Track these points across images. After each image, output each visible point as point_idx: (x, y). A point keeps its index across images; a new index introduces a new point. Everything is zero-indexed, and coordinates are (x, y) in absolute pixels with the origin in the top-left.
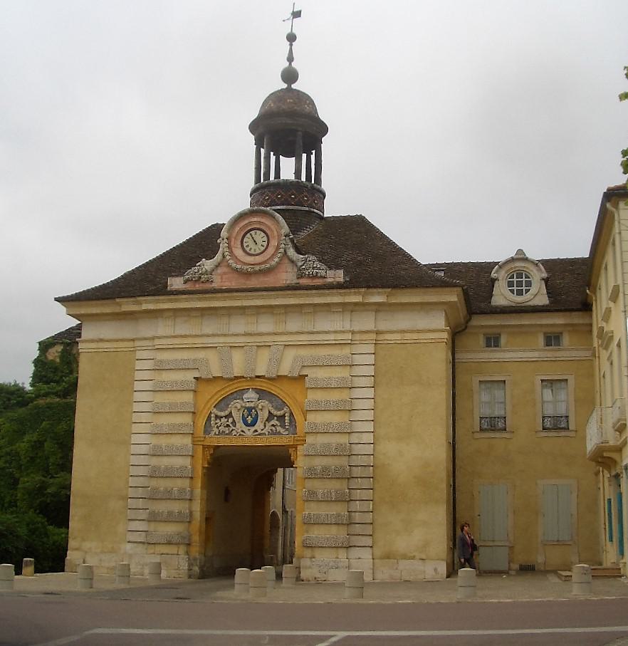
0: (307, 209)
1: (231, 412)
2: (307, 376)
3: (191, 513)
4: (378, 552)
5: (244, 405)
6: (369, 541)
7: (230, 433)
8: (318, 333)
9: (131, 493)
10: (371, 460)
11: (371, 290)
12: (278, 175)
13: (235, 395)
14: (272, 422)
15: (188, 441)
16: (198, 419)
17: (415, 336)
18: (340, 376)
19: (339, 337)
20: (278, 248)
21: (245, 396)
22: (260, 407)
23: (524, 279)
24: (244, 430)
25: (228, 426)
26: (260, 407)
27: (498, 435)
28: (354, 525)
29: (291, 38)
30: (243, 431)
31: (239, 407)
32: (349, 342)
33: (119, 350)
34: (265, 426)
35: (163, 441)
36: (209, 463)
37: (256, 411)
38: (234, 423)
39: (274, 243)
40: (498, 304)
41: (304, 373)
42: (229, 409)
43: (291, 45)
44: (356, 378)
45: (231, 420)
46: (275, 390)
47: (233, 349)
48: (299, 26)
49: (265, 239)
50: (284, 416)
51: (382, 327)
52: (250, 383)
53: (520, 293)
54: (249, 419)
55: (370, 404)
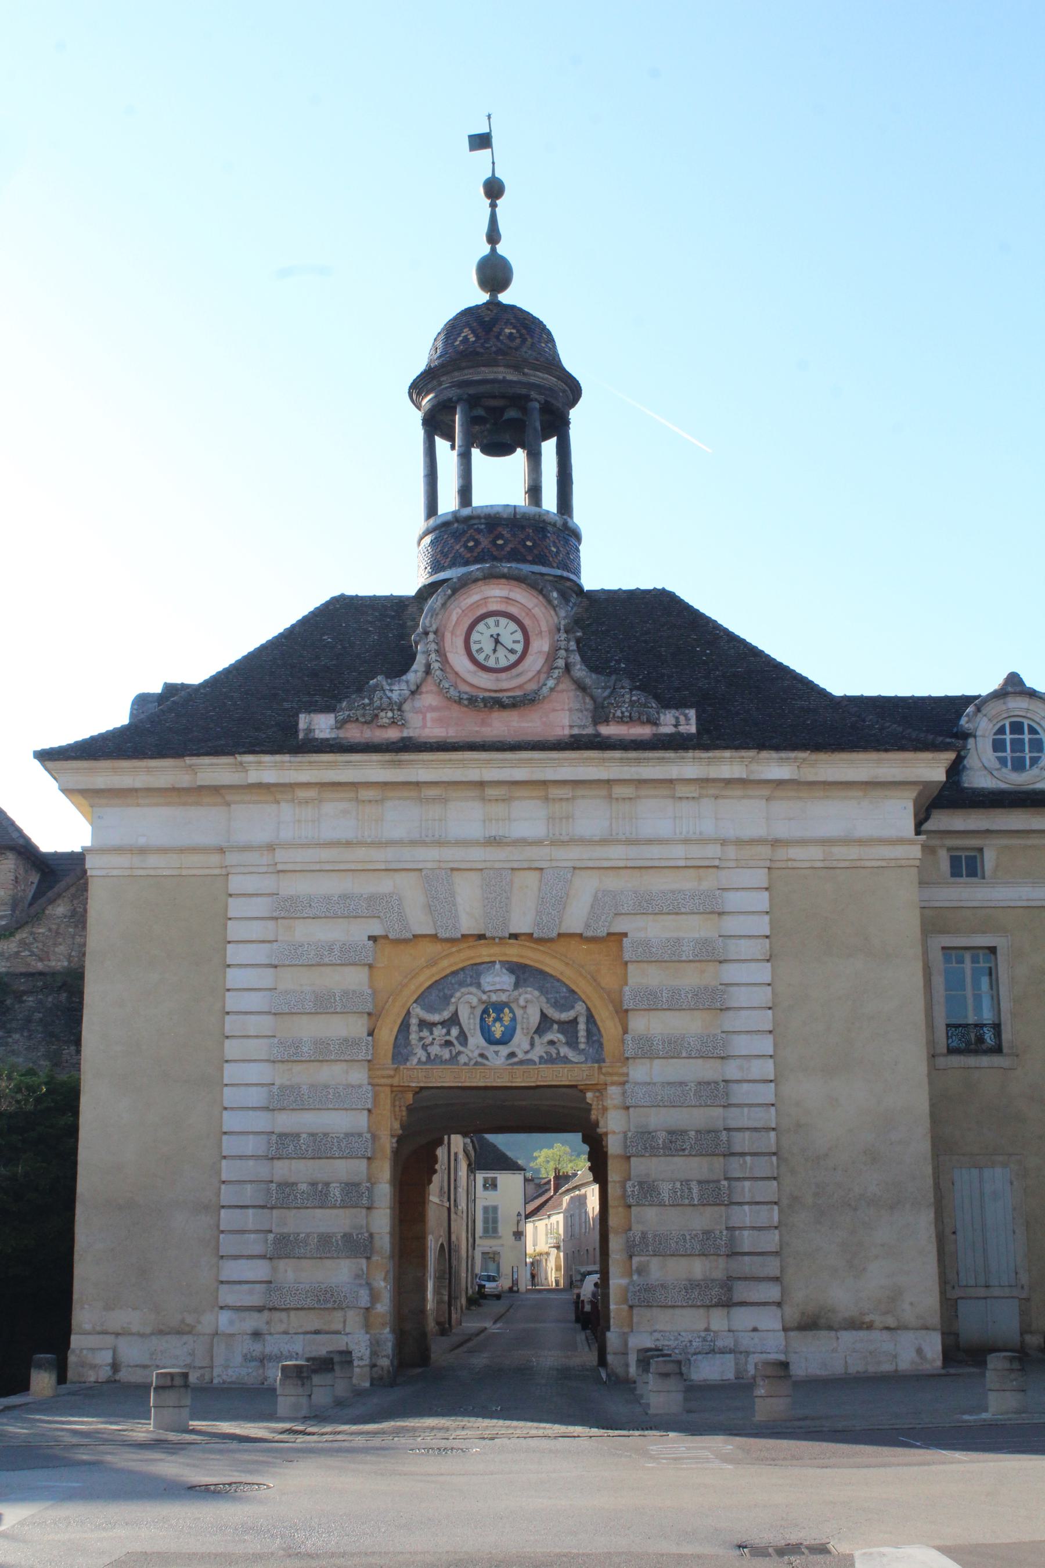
0: (559, 572)
1: (456, 1014)
2: (625, 935)
4: (792, 1313)
5: (484, 997)
6: (773, 1292)
7: (454, 1059)
8: (650, 842)
9: (227, 1195)
10: (770, 1117)
11: (764, 754)
12: (465, 492)
13: (461, 976)
14: (550, 1036)
15: (359, 1076)
17: (853, 853)
20: (551, 657)
22: (522, 1002)
23: (1026, 737)
24: (486, 1053)
25: (448, 1043)
27: (985, 1061)
28: (740, 1258)
29: (494, 189)
30: (482, 1055)
31: (474, 1001)
32: (716, 863)
33: (184, 872)
35: (302, 1075)
36: (402, 1127)
37: (512, 1011)
38: (463, 1038)
39: (541, 645)
40: (976, 785)
43: (493, 206)
45: (455, 1032)
46: (551, 965)
47: (455, 873)
49: (519, 636)
50: (575, 1021)
51: (782, 830)
53: (1019, 766)
54: (498, 1030)
55: (764, 996)
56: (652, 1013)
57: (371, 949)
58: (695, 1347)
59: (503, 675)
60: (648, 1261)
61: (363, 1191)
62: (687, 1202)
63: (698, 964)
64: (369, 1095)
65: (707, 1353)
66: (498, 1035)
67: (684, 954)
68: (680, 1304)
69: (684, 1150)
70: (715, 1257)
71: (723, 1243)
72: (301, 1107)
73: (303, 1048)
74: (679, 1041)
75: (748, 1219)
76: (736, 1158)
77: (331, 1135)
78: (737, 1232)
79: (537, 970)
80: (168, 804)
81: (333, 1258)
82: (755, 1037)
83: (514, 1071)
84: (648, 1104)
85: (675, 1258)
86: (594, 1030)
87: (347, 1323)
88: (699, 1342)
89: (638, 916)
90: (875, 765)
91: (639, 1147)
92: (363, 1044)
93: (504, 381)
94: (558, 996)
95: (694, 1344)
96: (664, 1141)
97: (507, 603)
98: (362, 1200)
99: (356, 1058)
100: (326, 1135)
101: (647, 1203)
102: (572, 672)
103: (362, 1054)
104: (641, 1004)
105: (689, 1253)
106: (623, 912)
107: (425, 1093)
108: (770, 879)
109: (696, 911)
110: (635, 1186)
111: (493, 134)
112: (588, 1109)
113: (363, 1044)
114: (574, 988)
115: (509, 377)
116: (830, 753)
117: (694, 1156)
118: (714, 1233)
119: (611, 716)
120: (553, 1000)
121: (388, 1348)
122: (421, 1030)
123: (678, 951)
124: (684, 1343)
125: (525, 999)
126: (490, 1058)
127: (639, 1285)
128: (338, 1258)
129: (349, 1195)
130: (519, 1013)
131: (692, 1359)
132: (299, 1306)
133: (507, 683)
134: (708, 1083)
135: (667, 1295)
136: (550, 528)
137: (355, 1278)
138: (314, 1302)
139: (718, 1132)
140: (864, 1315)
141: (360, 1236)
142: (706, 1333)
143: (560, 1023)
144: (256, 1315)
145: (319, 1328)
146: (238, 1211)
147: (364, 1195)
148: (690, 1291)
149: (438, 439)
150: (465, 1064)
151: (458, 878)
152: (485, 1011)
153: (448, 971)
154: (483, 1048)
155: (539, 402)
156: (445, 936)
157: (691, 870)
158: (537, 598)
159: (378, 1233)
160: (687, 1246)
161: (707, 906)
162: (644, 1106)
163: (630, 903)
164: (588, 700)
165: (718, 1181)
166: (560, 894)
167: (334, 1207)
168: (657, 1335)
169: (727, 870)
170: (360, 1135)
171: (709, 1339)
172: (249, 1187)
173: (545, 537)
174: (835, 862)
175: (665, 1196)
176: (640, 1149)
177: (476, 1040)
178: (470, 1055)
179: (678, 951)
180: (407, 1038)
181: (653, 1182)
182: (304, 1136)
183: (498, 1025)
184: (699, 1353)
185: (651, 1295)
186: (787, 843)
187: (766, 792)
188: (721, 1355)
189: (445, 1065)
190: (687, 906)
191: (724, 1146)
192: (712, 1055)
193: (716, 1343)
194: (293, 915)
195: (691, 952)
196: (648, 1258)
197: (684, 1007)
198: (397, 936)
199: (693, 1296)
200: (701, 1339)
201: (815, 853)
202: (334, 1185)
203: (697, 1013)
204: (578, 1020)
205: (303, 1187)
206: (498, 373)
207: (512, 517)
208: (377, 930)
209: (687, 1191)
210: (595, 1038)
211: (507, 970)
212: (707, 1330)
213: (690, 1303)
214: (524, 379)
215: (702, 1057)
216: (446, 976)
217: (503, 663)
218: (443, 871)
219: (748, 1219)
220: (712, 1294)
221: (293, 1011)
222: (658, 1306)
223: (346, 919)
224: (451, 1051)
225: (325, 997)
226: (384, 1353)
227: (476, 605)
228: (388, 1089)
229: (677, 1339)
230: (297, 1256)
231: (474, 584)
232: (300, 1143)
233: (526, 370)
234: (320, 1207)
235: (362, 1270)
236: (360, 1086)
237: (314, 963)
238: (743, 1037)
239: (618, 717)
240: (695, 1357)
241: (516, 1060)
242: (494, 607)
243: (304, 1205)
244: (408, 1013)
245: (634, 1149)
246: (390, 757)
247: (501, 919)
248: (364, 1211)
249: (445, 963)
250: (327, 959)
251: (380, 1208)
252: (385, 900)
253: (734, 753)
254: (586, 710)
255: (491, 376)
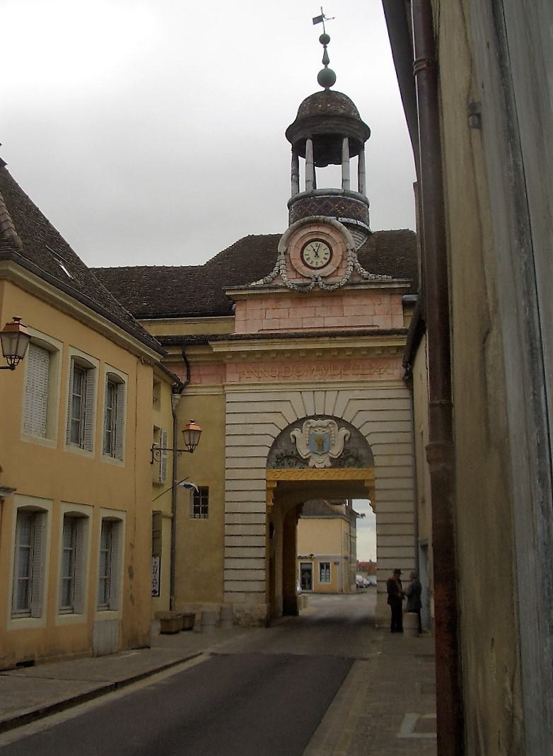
29: (325, 40)
43: (325, 47)
48: (329, 27)
149: (299, 157)
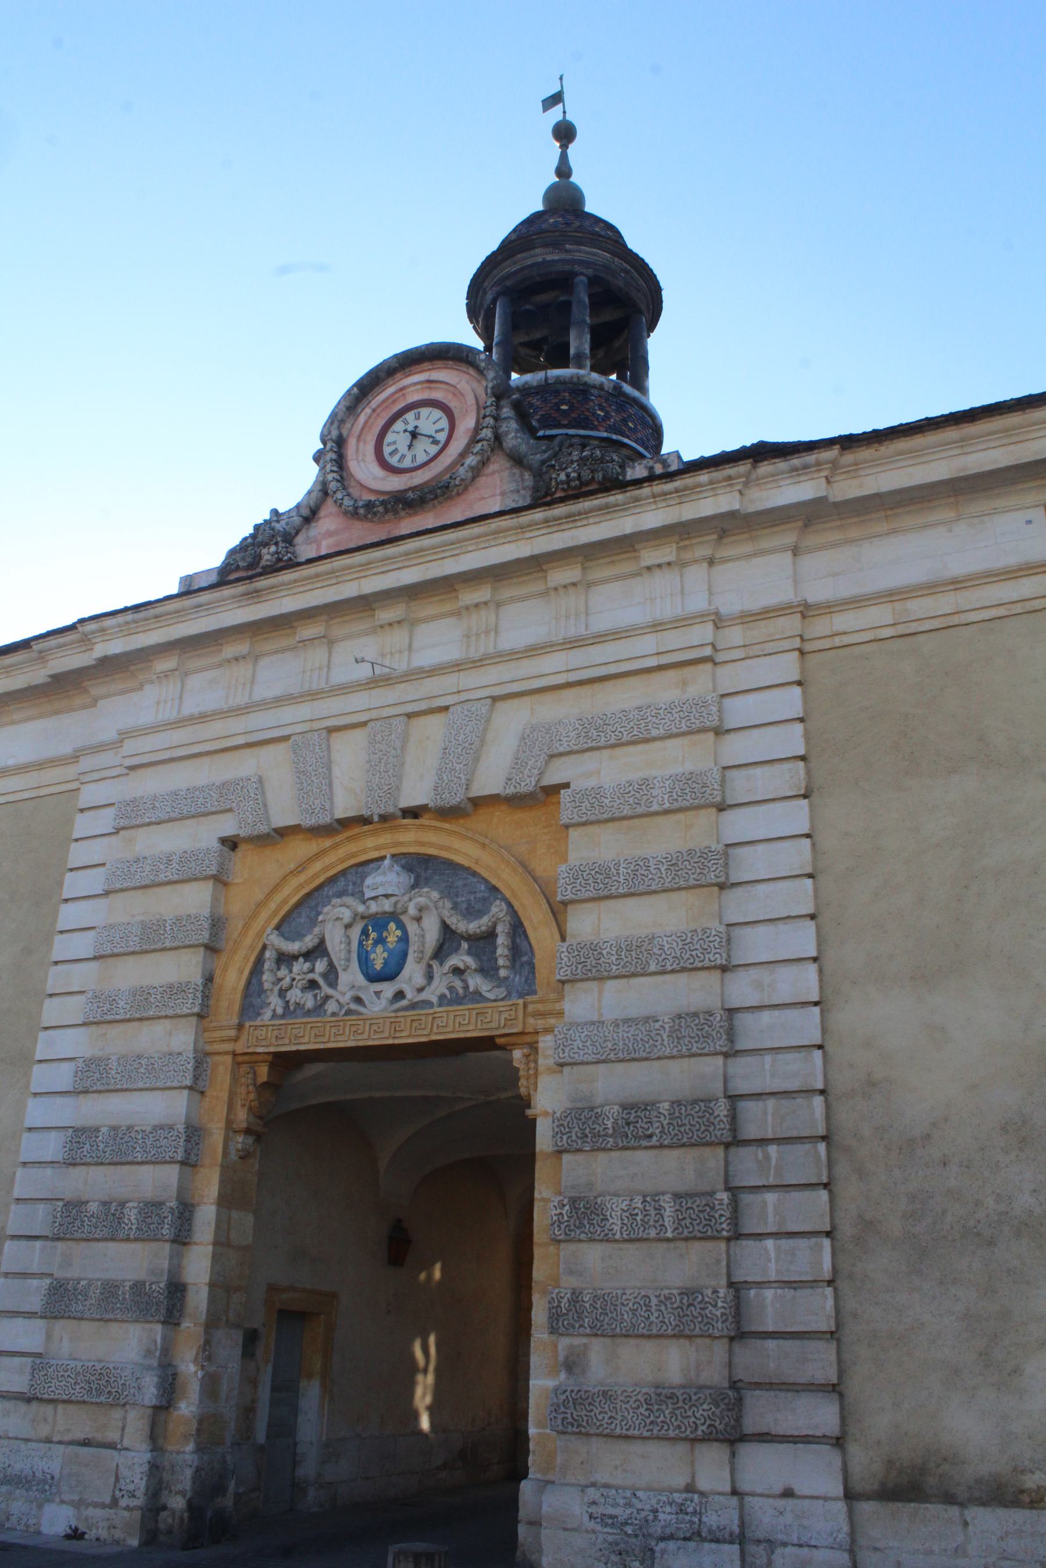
2: (567, 786)
3: (177, 1289)
5: (361, 908)
7: (319, 1008)
8: (601, 638)
9: (16, 1220)
13: (341, 883)
14: (454, 961)
16: (225, 970)
17: (945, 603)
18: (680, 770)
19: (673, 639)
20: (477, 429)
21: (369, 881)
22: (412, 911)
25: (313, 985)
26: (412, 911)
28: (758, 1343)
29: (565, 133)
33: (43, 792)
34: (430, 977)
38: (331, 975)
39: (467, 423)
41: (552, 778)
42: (316, 930)
44: (743, 773)
45: (321, 966)
47: (335, 735)
49: (444, 423)
50: (490, 935)
51: (817, 592)
52: (385, 838)
54: (379, 958)
56: (605, 905)
57: (216, 855)
58: (663, 1523)
59: (420, 472)
60: (585, 1345)
61: (166, 1214)
62: (653, 1233)
63: (680, 817)
64: (189, 1066)
65: (685, 1539)
66: (378, 966)
67: (655, 800)
68: (636, 1432)
69: (650, 1136)
70: (707, 1341)
71: (718, 1313)
72: (106, 1087)
73: (120, 1001)
74: (646, 944)
75: (772, 1265)
76: (752, 1149)
77: (136, 1128)
78: (752, 1292)
79: (444, 863)
80: (41, 716)
81: (116, 1320)
82: (781, 926)
83: (399, 1020)
84: (590, 1059)
85: (632, 1341)
86: (524, 946)
87: (127, 1431)
88: (669, 1513)
89: (588, 754)
90: (959, 451)
91: (573, 1135)
92: (191, 991)
93: (544, 262)
94: (472, 898)
95: (661, 1516)
96: (615, 1122)
97: (430, 388)
98: (162, 1228)
99: (179, 1012)
100: (129, 1128)
101: (583, 1236)
102: (504, 444)
103: (188, 1005)
104: (583, 890)
105: (654, 1332)
106: (561, 749)
107: (313, 1069)
108: (803, 670)
109: (675, 731)
110: (564, 1206)
111: (564, 90)
112: (513, 1076)
113: (191, 991)
114: (494, 882)
115: (549, 258)
116: (876, 445)
117: (669, 1147)
118: (703, 1296)
119: (553, 483)
120: (464, 906)
121: (185, 1480)
122: (279, 969)
123: (645, 797)
124: (643, 1514)
125: (416, 904)
126: (366, 1002)
127: (565, 1391)
128: (123, 1321)
129: (147, 1220)
130: (412, 928)
131: (657, 1549)
132: (65, 1397)
133: (420, 478)
134: (695, 1015)
135: (613, 1414)
136: (595, 392)
137: (145, 1356)
138: (84, 1391)
139: (710, 1101)
140: (1023, 1472)
141: (154, 1287)
142: (684, 1495)
143: (470, 938)
144: (22, 1407)
145: (90, 1436)
146: (24, 1243)
147: (166, 1221)
148: (656, 1407)
150: (334, 1014)
151: (338, 741)
152: (365, 933)
153: (322, 879)
154: (360, 988)
155: (586, 275)
156: (310, 823)
157: (671, 674)
158: (468, 373)
159: (194, 1284)
160: (653, 1318)
161: (693, 721)
162: (582, 1063)
163: (572, 734)
164: (527, 475)
165: (711, 1194)
166: (469, 738)
167: (128, 1240)
168: (592, 1494)
169: (730, 665)
170: (171, 1128)
171: (690, 1510)
172: (41, 1207)
173: (587, 400)
174: (913, 624)
175: (615, 1223)
176: (574, 1138)
177: (351, 977)
178: (341, 1000)
179: (645, 797)
180: (261, 984)
181: (595, 1197)
182: (104, 1130)
183: (379, 949)
184: (671, 1537)
185: (584, 1412)
186: (829, 607)
187: (788, 537)
188: (713, 1545)
189: (310, 1017)
190: (660, 726)
191: (722, 1126)
192: (700, 965)
193: (704, 1519)
194: (134, 822)
195: (666, 797)
196: (585, 1340)
197: (653, 887)
198: (250, 833)
199: (662, 1418)
200: (674, 1509)
201: (880, 615)
202: (130, 1204)
203: (675, 896)
204: (497, 931)
205: (93, 1207)
206: (536, 256)
207: (543, 383)
208: (228, 826)
209: (653, 1212)
210: (525, 959)
211: (403, 867)
212: (690, 1488)
213: (655, 1432)
214: (568, 257)
215: (683, 970)
216: (320, 887)
217: (422, 458)
218: (316, 734)
219: (772, 1265)
220: (698, 1415)
221: (116, 951)
222: (597, 1435)
223: (195, 820)
224: (315, 996)
225: (154, 928)
226: (180, 1487)
227: (392, 399)
228: (229, 1059)
229: (629, 1505)
230: (72, 1315)
231: (391, 379)
232: (98, 1140)
233: (568, 246)
234: (112, 1239)
235: (155, 1341)
236: (180, 1054)
237: (147, 882)
238: (761, 929)
239: (562, 482)
240: (662, 1545)
241: (404, 1003)
242: (413, 397)
243: (91, 1236)
244: (264, 947)
245: (565, 1137)
246: (244, 587)
247: (386, 788)
248: (167, 1246)
249: (318, 866)
250: (162, 876)
251: (201, 1244)
252: (241, 785)
253: (715, 474)
254: (524, 489)
255: (529, 262)
